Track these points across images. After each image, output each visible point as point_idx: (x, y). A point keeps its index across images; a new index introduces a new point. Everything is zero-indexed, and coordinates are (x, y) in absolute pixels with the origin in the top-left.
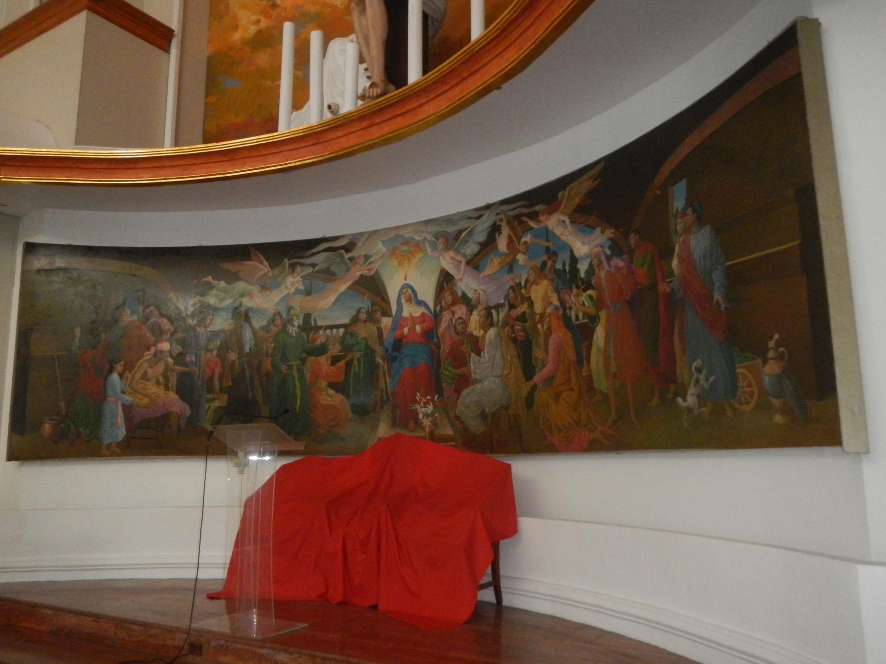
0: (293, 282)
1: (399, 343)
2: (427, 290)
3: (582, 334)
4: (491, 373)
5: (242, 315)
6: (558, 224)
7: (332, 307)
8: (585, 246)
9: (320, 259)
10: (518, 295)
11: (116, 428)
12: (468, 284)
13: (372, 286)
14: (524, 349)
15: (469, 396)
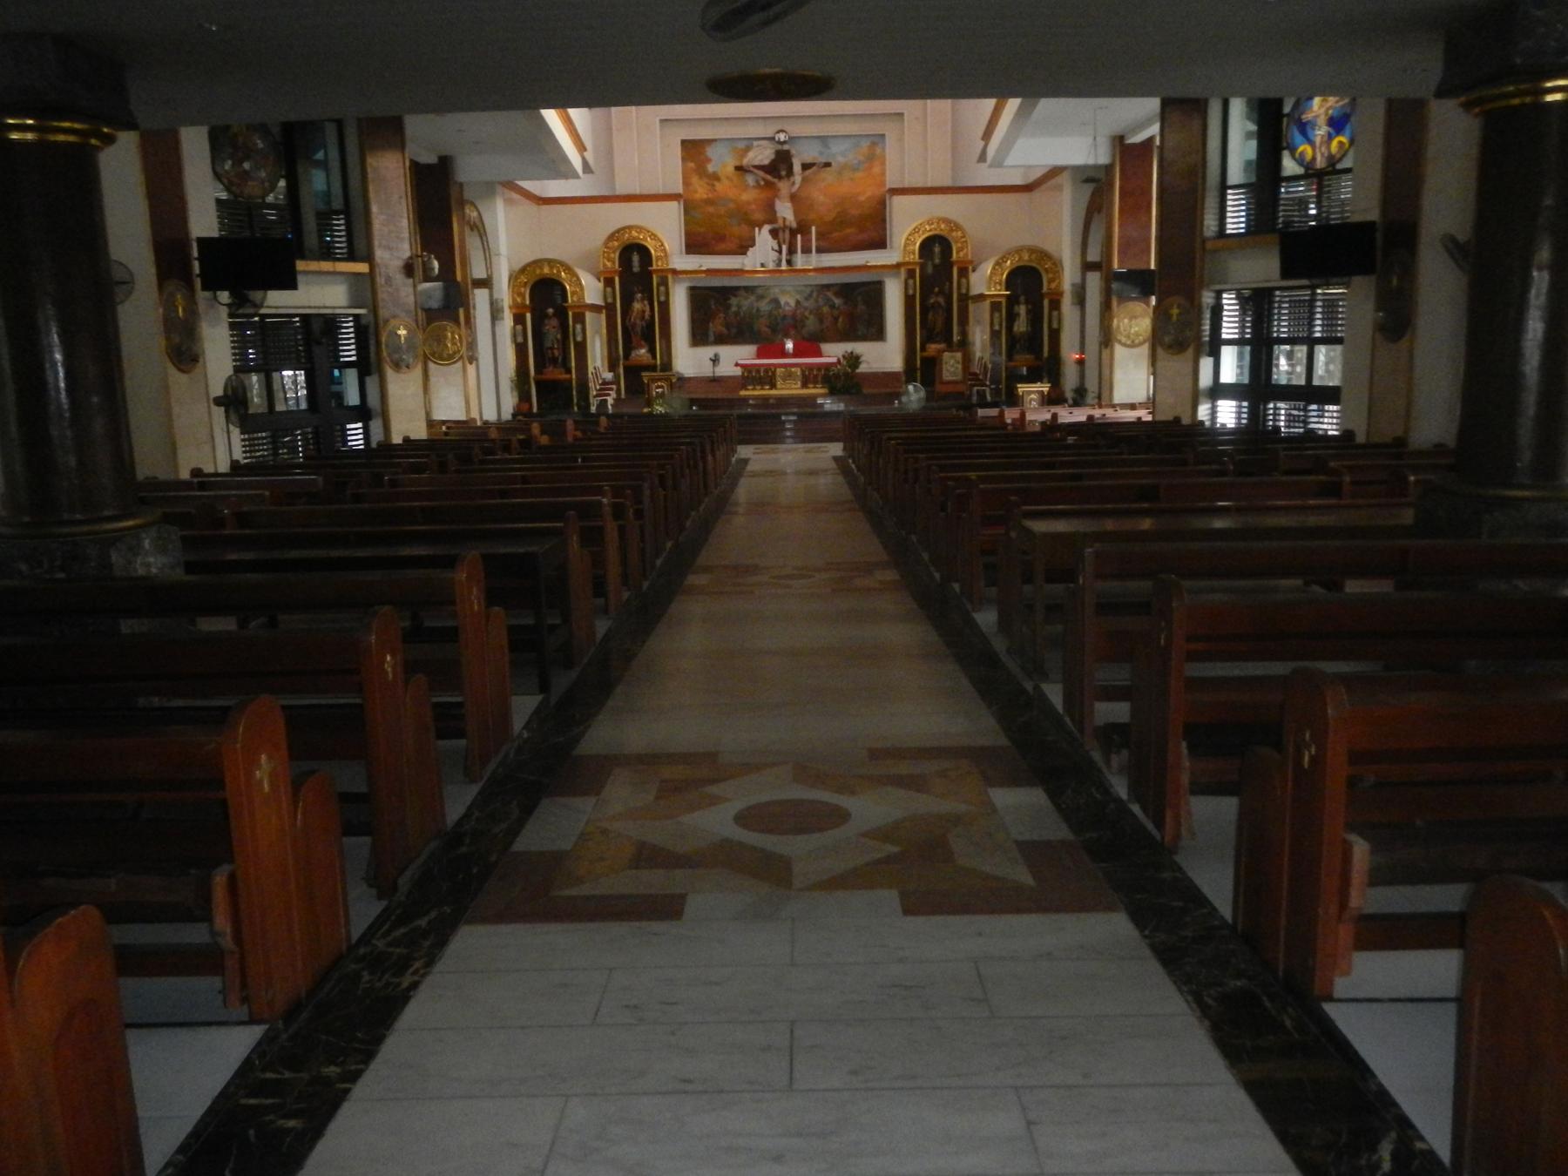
0: (753, 298)
1: (785, 317)
2: (793, 303)
3: (836, 319)
4: (812, 323)
5: (739, 307)
6: (830, 294)
7: (764, 306)
8: (837, 301)
9: (760, 291)
10: (819, 308)
11: (712, 338)
12: (806, 304)
13: (776, 301)
14: (821, 321)
15: (804, 331)
